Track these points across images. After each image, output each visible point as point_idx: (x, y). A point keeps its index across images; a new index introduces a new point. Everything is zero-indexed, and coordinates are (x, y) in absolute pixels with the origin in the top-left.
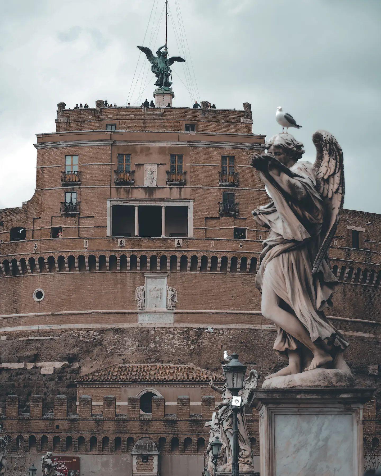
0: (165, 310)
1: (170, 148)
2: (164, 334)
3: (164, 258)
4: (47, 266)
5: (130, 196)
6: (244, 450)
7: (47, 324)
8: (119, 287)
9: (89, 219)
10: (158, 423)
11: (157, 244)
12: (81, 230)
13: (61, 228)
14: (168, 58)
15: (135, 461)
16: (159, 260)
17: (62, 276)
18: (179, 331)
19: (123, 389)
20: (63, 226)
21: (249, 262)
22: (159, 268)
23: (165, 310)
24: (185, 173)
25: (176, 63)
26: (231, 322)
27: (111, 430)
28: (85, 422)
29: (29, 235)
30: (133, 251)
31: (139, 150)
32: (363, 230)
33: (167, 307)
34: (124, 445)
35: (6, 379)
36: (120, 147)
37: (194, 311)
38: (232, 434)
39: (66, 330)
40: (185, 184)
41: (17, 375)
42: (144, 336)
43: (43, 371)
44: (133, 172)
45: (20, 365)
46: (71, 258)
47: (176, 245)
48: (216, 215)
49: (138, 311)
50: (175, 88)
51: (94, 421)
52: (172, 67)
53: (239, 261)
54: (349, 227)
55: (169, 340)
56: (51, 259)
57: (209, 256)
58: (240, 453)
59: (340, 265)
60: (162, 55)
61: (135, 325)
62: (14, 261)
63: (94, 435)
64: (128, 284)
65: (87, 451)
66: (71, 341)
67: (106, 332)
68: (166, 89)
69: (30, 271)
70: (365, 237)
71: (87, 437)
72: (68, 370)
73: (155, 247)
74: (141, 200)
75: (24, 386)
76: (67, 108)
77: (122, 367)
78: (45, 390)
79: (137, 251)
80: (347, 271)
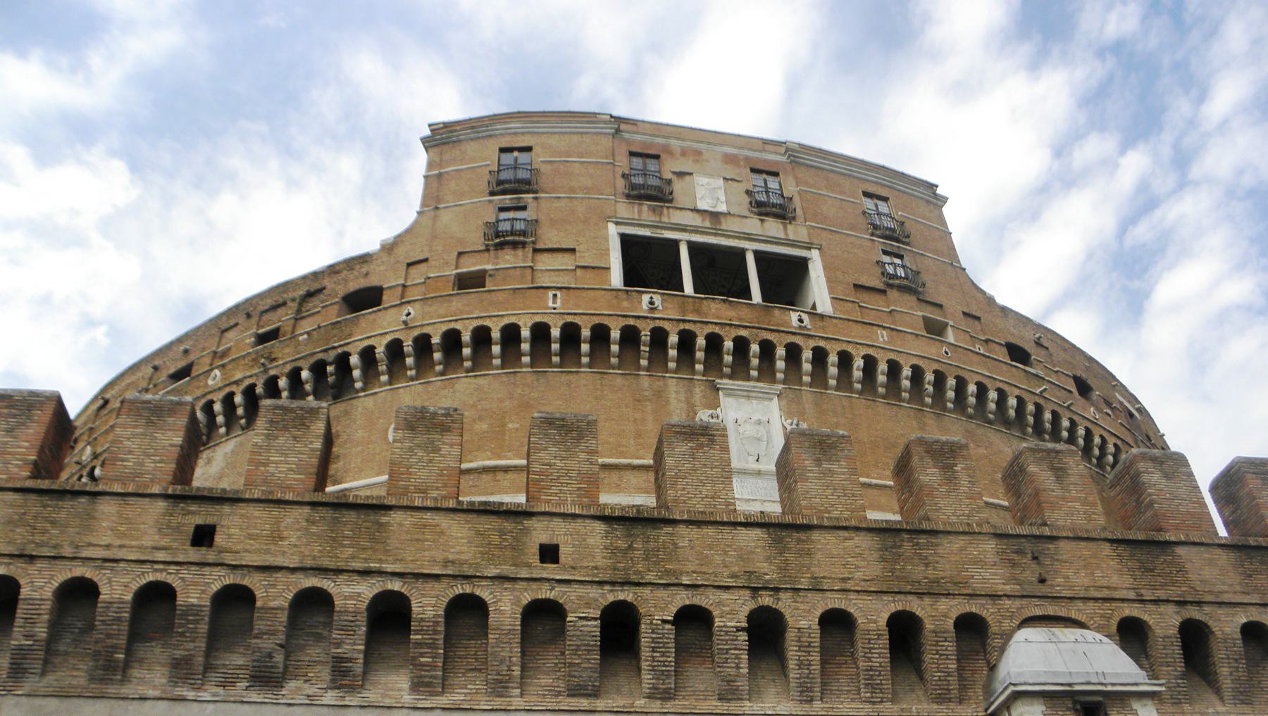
1: (747, 159)
8: (649, 407)
9: (559, 256)
10: (1085, 549)
11: (745, 313)
12: (538, 275)
13: (485, 271)
17: (481, 381)
20: (489, 267)
22: (754, 373)
27: (858, 575)
28: (710, 531)
29: (387, 299)
30: (684, 321)
40: (794, 218)
44: (669, 182)
46: (511, 334)
47: (795, 322)
51: (757, 533)
62: (343, 360)
63: (766, 600)
64: (673, 402)
71: (731, 613)
73: (740, 320)
79: (695, 322)
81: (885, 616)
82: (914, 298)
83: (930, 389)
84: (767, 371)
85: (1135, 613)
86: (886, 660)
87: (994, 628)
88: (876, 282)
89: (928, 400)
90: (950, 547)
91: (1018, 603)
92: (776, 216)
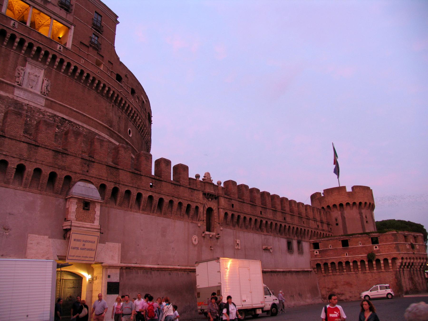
0: (39, 93)
2: (36, 112)
3: (47, 54)
15: (73, 207)
18: (49, 114)
22: (40, 60)
23: (39, 93)
24: (72, 5)
26: (84, 122)
28: (14, 142)
33: (41, 92)
34: (59, 183)
37: (61, 103)
40: (71, 12)
49: (16, 84)
55: (39, 118)
61: (11, 96)
63: (23, 162)
73: (41, 41)
79: (27, 37)
81: (50, 172)
82: (96, 52)
83: (90, 82)
84: (44, 61)
85: (105, 183)
86: (46, 182)
87: (73, 180)
88: (87, 43)
89: (88, 85)
90: (70, 159)
91: (80, 175)
92: (66, 10)
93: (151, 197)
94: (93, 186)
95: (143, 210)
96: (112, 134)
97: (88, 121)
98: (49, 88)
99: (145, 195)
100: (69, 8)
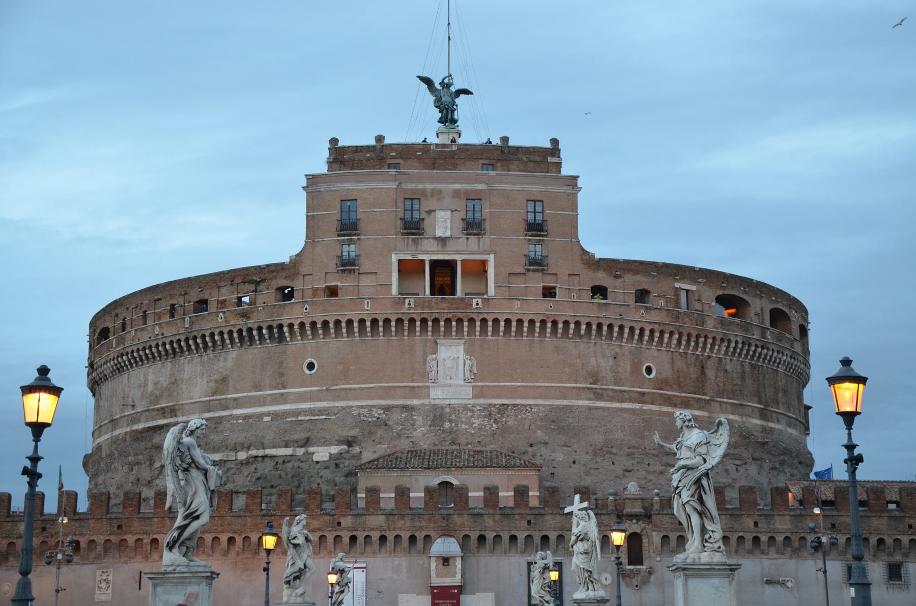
1: (467, 192)
3: (460, 321)
4: (320, 332)
5: (419, 247)
6: (713, 531)
7: (320, 400)
13: (337, 286)
14: (453, 89)
15: (433, 565)
16: (454, 323)
19: (414, 478)
20: (339, 284)
21: (561, 325)
22: (454, 334)
23: (462, 382)
25: (462, 96)
26: (541, 397)
31: (429, 194)
32: (693, 288)
34: (420, 543)
35: (271, 468)
36: (407, 190)
38: (696, 509)
39: (343, 408)
41: (284, 462)
42: (438, 415)
43: (316, 458)
44: (423, 219)
45: (288, 451)
46: (350, 322)
48: (521, 270)
49: (430, 384)
50: (462, 124)
52: (457, 101)
53: (549, 325)
54: (677, 285)
56: (326, 323)
57: (514, 319)
58: (707, 536)
59: (667, 329)
60: (446, 86)
61: (426, 402)
62: (280, 327)
63: (383, 533)
65: (374, 553)
66: (350, 421)
67: (392, 410)
68: (453, 126)
69: (299, 338)
70: (696, 297)
71: (375, 536)
72: (346, 455)
74: (433, 253)
75: (293, 476)
76: (340, 144)
77: (412, 452)
78: (319, 481)
80: (676, 336)
82: (541, 274)
92: (475, 235)
93: (529, 537)
94: (453, 540)
95: (521, 552)
96: (599, 396)
97: (546, 393)
98: (474, 370)
99: (521, 536)
100: (481, 229)
